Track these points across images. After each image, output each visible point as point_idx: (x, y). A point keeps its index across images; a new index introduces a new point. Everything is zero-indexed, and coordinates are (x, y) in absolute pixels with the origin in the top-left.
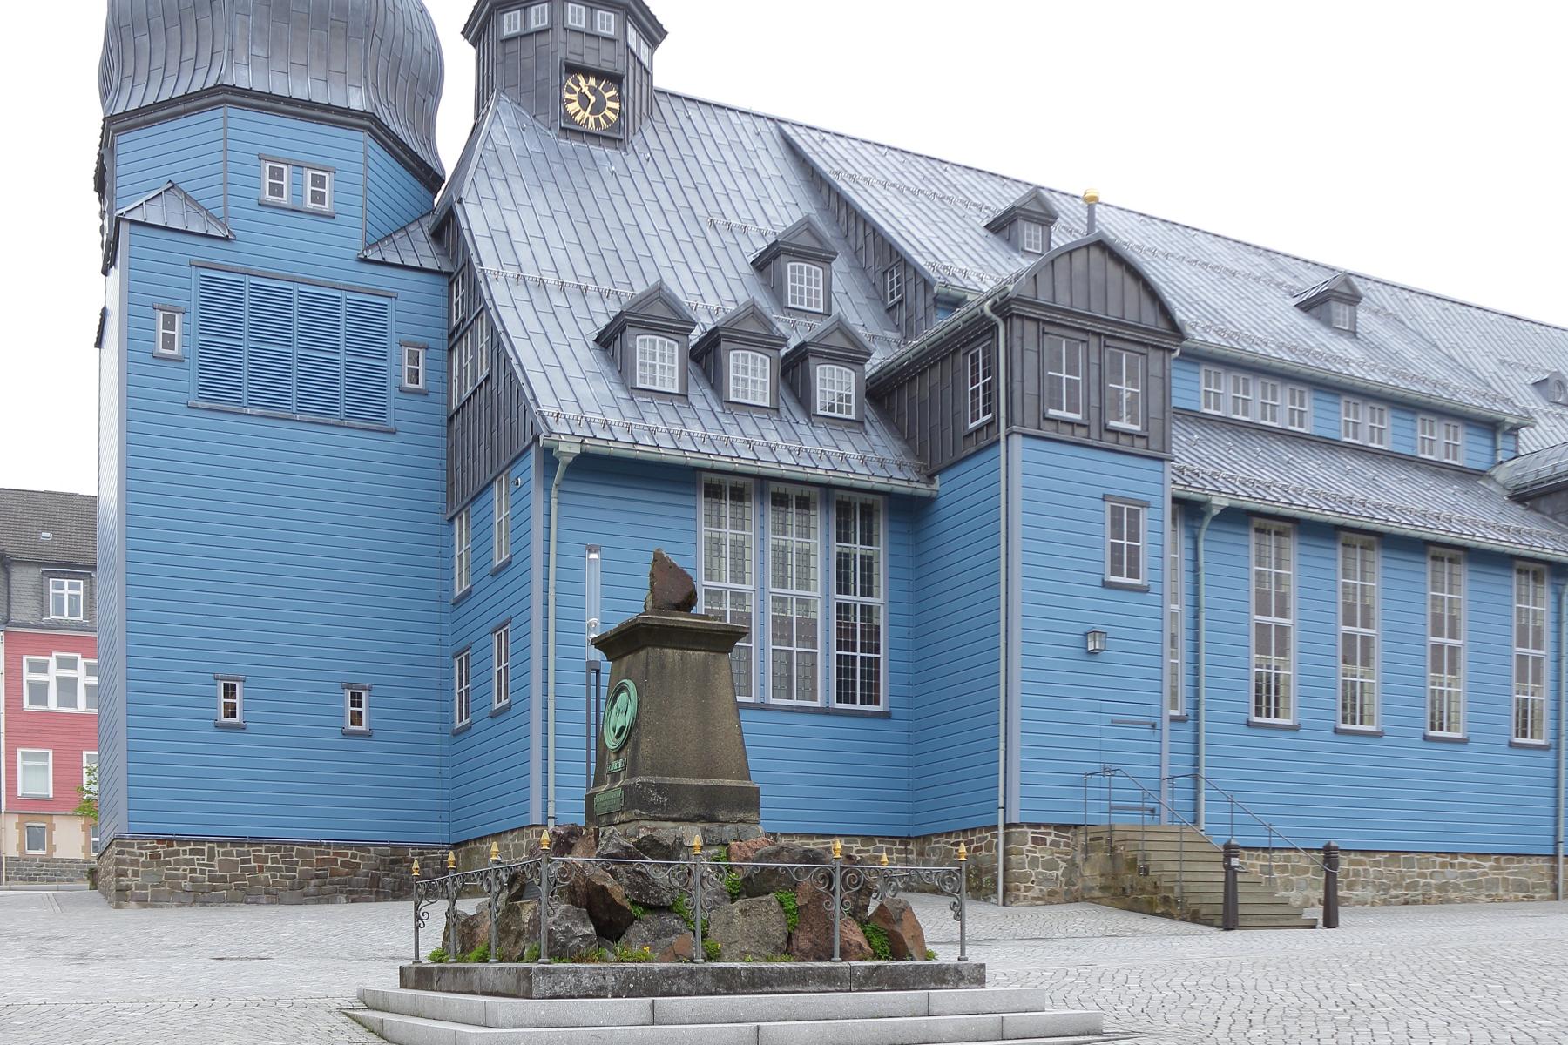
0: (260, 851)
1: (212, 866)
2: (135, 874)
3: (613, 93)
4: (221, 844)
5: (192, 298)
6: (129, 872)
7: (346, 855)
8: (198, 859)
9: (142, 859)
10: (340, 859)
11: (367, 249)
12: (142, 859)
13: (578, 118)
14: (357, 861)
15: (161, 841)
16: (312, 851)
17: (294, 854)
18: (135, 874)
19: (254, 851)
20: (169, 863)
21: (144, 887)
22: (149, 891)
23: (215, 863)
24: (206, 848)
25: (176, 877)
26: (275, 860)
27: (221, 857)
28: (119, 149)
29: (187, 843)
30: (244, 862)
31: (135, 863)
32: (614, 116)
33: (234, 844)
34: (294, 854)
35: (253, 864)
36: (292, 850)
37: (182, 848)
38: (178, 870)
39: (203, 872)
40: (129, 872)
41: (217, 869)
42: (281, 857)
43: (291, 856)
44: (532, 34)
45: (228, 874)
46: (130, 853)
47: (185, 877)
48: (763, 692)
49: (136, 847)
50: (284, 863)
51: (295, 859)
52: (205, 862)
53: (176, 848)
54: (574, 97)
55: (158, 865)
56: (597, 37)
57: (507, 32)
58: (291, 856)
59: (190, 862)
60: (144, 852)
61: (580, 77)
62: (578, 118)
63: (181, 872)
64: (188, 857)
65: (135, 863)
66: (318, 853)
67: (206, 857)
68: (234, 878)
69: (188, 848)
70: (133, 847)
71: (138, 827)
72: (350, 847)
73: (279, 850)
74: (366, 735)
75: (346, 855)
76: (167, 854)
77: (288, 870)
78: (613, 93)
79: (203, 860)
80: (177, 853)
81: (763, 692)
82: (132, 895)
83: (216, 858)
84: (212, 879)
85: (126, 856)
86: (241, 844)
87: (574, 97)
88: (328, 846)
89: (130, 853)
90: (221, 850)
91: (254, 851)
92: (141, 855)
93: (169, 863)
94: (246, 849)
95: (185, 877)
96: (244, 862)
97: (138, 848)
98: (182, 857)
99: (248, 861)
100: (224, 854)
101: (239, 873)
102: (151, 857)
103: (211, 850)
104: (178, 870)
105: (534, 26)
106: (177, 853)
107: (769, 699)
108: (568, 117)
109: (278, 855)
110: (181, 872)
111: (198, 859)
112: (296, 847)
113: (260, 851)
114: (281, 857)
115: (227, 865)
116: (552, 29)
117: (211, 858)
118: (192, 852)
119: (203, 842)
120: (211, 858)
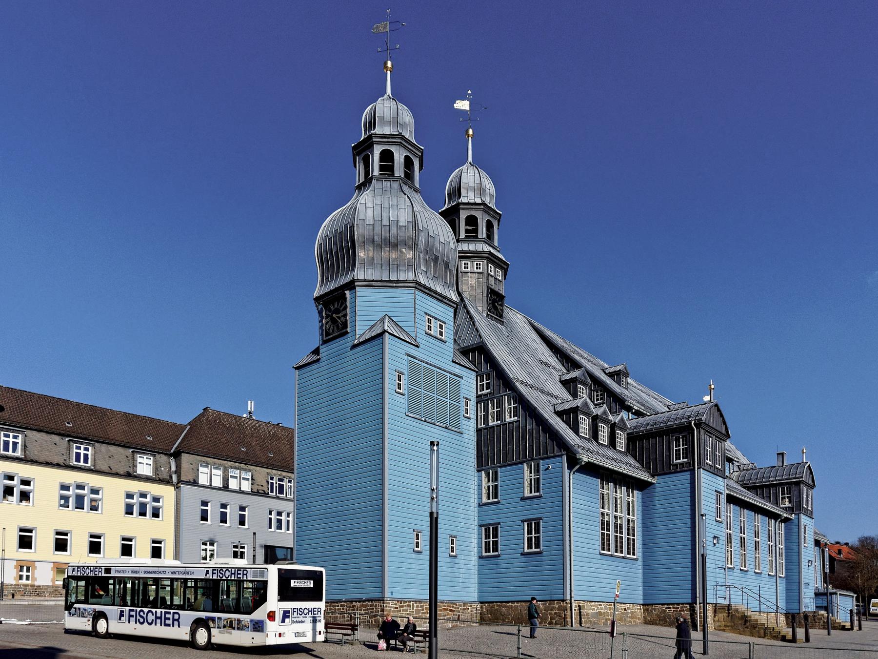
1: (413, 612)
4: (416, 602)
5: (405, 368)
7: (450, 607)
10: (449, 608)
12: (392, 609)
14: (454, 609)
15: (398, 601)
29: (405, 602)
33: (420, 602)
35: (425, 611)
38: (403, 614)
46: (389, 607)
53: (402, 604)
59: (406, 610)
64: (406, 608)
66: (444, 606)
69: (406, 604)
70: (389, 604)
72: (452, 603)
74: (455, 556)
75: (450, 607)
80: (403, 606)
88: (446, 603)
90: (416, 605)
93: (400, 611)
98: (404, 608)
99: (423, 610)
102: (395, 608)
103: (413, 604)
104: (403, 614)
106: (403, 606)
110: (404, 615)
117: (413, 609)
119: (410, 602)
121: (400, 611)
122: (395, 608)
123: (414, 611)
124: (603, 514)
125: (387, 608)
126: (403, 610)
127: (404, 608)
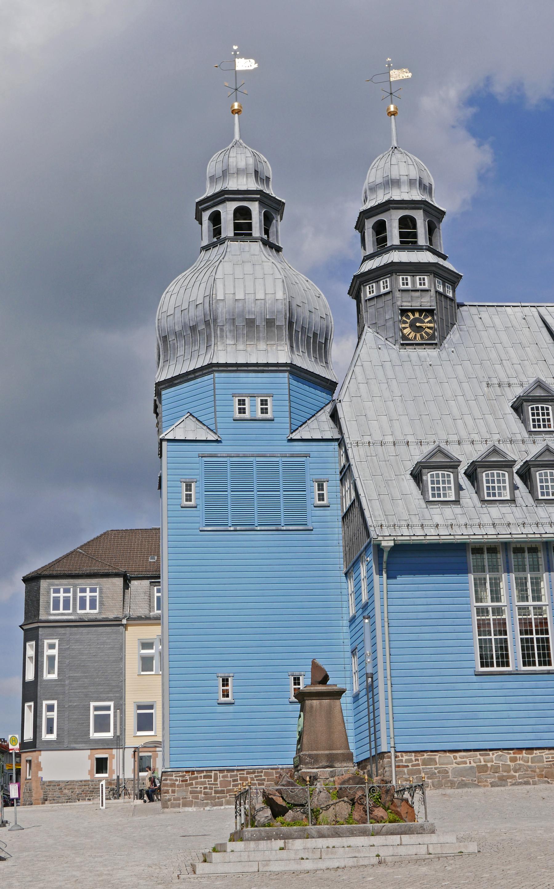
0: (243, 774)
2: (173, 792)
3: (430, 318)
4: (221, 771)
6: (170, 791)
8: (208, 781)
9: (177, 783)
11: (292, 433)
12: (177, 783)
13: (410, 336)
15: (187, 772)
16: (273, 773)
17: (263, 774)
18: (173, 792)
19: (240, 774)
20: (191, 784)
21: (178, 799)
22: (181, 801)
23: (218, 782)
24: (213, 774)
25: (196, 792)
26: (252, 779)
27: (221, 779)
28: (163, 397)
30: (234, 781)
31: (173, 785)
32: (431, 331)
33: (228, 771)
34: (263, 774)
36: (262, 772)
37: (199, 775)
38: (197, 788)
39: (211, 788)
40: (170, 791)
41: (219, 786)
42: (256, 777)
43: (261, 776)
44: (382, 295)
45: (225, 789)
46: (171, 780)
47: (201, 792)
48: (516, 663)
49: (174, 776)
50: (257, 780)
51: (263, 777)
52: (213, 782)
53: (196, 775)
54: (407, 325)
55: (187, 785)
56: (418, 290)
57: (369, 296)
58: (261, 776)
59: (204, 783)
60: (178, 778)
61: (410, 314)
62: (410, 336)
63: (199, 789)
64: (203, 780)
65: (173, 785)
67: (213, 779)
68: (229, 791)
69: (202, 775)
71: (174, 764)
73: (254, 773)
76: (191, 779)
77: (259, 784)
78: (430, 318)
79: (211, 781)
80: (196, 778)
81: (516, 663)
82: (172, 804)
83: (219, 780)
84: (216, 792)
85: (168, 782)
86: (233, 771)
87: (407, 325)
89: (171, 780)
90: (221, 775)
91: (240, 774)
92: (177, 780)
93: (192, 784)
94: (235, 773)
95: (201, 792)
96: (234, 781)
97: (175, 777)
98: (199, 780)
100: (223, 777)
101: (231, 788)
102: (182, 781)
103: (216, 775)
104: (197, 788)
105: (383, 291)
106: (196, 778)
107: (520, 667)
108: (404, 337)
109: (253, 776)
111: (208, 781)
112: (264, 770)
113: (243, 774)
114: (256, 777)
115: (225, 783)
116: (391, 291)
117: (216, 780)
118: (205, 777)
120: (216, 780)
121: (192, 784)
122: (182, 781)
123: (218, 782)
124: (482, 611)
125: (168, 782)
126: (196, 784)
127: (199, 780)
